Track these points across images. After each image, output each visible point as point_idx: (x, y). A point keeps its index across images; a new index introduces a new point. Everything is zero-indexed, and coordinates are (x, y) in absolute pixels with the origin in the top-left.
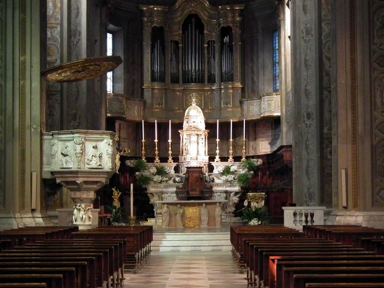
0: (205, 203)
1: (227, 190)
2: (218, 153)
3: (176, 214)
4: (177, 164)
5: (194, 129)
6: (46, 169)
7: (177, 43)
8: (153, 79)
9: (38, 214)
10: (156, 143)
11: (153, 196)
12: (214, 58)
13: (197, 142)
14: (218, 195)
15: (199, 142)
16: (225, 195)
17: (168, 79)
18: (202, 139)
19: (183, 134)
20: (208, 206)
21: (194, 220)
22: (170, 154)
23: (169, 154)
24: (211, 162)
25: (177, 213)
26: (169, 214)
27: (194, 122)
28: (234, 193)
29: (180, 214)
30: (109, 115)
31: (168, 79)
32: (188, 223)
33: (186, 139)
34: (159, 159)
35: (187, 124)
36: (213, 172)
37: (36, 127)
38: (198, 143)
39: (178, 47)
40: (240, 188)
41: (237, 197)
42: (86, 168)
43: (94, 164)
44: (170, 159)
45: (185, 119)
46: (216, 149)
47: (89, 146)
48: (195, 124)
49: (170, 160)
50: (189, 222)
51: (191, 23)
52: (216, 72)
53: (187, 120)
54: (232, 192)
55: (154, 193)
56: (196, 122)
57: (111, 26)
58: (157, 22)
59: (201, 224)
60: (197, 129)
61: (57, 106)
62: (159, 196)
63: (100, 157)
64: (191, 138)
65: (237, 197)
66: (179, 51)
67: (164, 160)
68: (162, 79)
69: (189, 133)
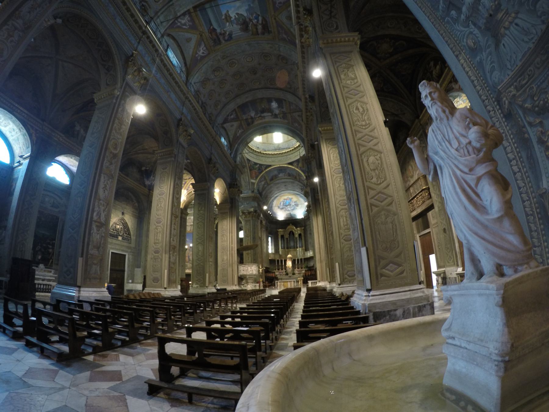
6: (239, 274)
7: (287, 239)
9: (237, 286)
17: (286, 248)
31: (286, 248)
37: (236, 263)
42: (248, 274)
43: (251, 273)
47: (249, 268)
52: (298, 246)
57: (270, 235)
58: (282, 233)
61: (250, 258)
63: (253, 270)
67: (282, 269)
68: (284, 248)
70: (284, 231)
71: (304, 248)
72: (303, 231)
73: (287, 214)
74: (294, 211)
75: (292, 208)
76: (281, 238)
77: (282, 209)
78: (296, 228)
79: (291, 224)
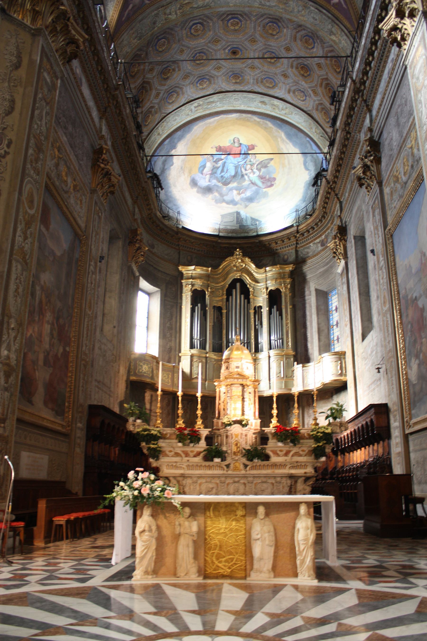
0: (267, 505)
1: (292, 474)
2: (275, 415)
3: (177, 537)
4: (209, 431)
5: (238, 376)
7: (219, 309)
8: (192, 346)
10: (180, 399)
11: (170, 481)
12: (261, 324)
13: (242, 398)
14: (277, 482)
15: (245, 397)
16: (289, 482)
18: (250, 393)
19: (220, 385)
20: (275, 517)
21: (231, 553)
22: (199, 415)
23: (197, 415)
24: (263, 429)
25: (180, 533)
26: (156, 535)
27: (237, 367)
28: (303, 478)
29: (187, 536)
30: (133, 378)
32: (213, 562)
33: (225, 393)
34: (183, 422)
35: (227, 371)
36: (267, 445)
38: (243, 399)
39: (221, 314)
40: (313, 471)
41: (309, 485)
44: (198, 423)
45: (225, 362)
46: (273, 408)
48: (239, 370)
49: (199, 425)
50: (217, 559)
51: (235, 288)
53: (226, 364)
54: (301, 477)
55: (170, 477)
56: (240, 367)
58: (199, 284)
59: (252, 569)
60: (242, 376)
62: (178, 482)
64: (233, 390)
65: (309, 485)
66: (222, 318)
69: (229, 381)
70: (207, 277)
71: (292, 353)
72: (288, 281)
73: (223, 216)
74: (252, 205)
75: (248, 194)
76: (194, 303)
77: (208, 190)
78: (259, 266)
79: (238, 252)
